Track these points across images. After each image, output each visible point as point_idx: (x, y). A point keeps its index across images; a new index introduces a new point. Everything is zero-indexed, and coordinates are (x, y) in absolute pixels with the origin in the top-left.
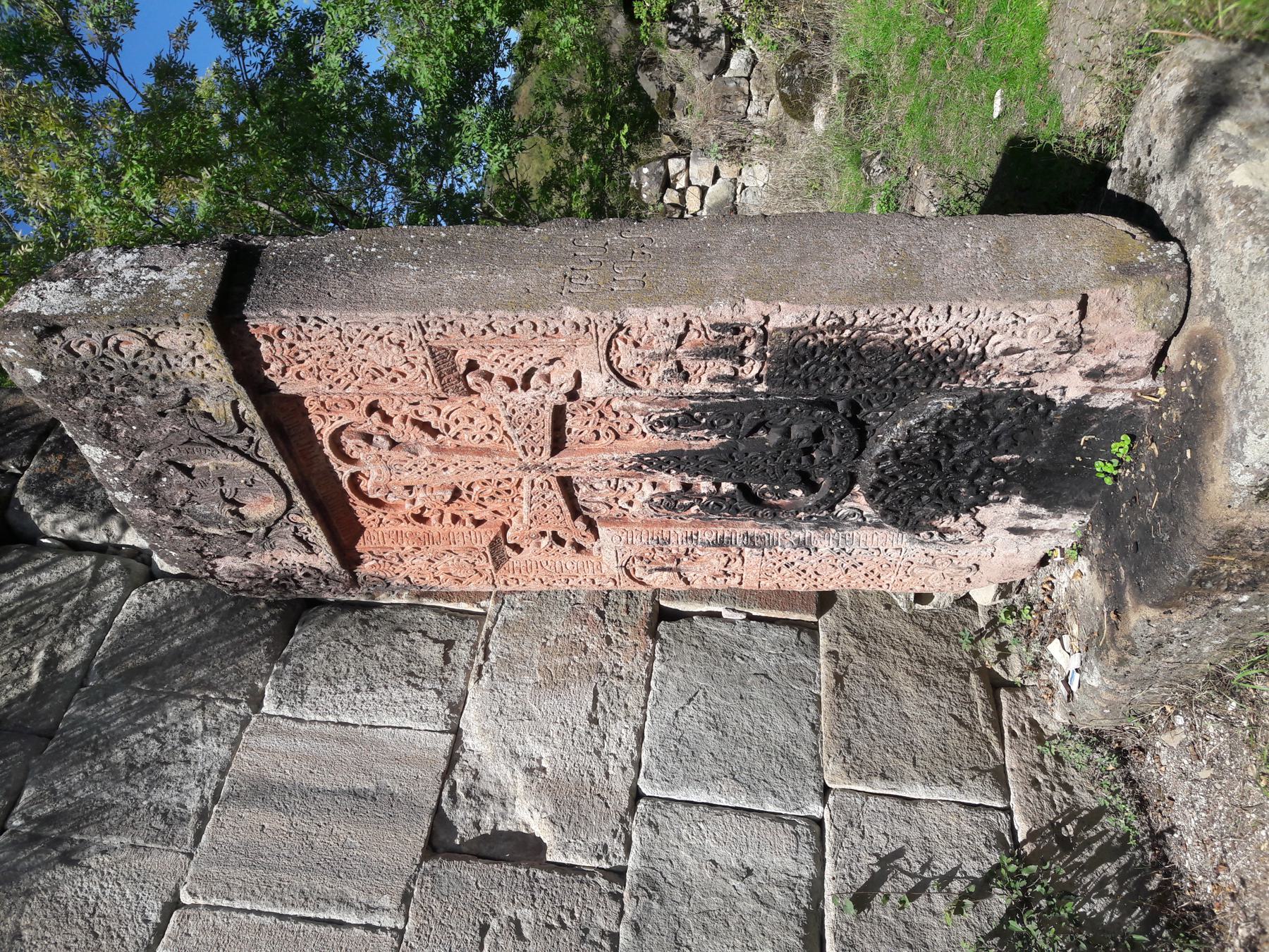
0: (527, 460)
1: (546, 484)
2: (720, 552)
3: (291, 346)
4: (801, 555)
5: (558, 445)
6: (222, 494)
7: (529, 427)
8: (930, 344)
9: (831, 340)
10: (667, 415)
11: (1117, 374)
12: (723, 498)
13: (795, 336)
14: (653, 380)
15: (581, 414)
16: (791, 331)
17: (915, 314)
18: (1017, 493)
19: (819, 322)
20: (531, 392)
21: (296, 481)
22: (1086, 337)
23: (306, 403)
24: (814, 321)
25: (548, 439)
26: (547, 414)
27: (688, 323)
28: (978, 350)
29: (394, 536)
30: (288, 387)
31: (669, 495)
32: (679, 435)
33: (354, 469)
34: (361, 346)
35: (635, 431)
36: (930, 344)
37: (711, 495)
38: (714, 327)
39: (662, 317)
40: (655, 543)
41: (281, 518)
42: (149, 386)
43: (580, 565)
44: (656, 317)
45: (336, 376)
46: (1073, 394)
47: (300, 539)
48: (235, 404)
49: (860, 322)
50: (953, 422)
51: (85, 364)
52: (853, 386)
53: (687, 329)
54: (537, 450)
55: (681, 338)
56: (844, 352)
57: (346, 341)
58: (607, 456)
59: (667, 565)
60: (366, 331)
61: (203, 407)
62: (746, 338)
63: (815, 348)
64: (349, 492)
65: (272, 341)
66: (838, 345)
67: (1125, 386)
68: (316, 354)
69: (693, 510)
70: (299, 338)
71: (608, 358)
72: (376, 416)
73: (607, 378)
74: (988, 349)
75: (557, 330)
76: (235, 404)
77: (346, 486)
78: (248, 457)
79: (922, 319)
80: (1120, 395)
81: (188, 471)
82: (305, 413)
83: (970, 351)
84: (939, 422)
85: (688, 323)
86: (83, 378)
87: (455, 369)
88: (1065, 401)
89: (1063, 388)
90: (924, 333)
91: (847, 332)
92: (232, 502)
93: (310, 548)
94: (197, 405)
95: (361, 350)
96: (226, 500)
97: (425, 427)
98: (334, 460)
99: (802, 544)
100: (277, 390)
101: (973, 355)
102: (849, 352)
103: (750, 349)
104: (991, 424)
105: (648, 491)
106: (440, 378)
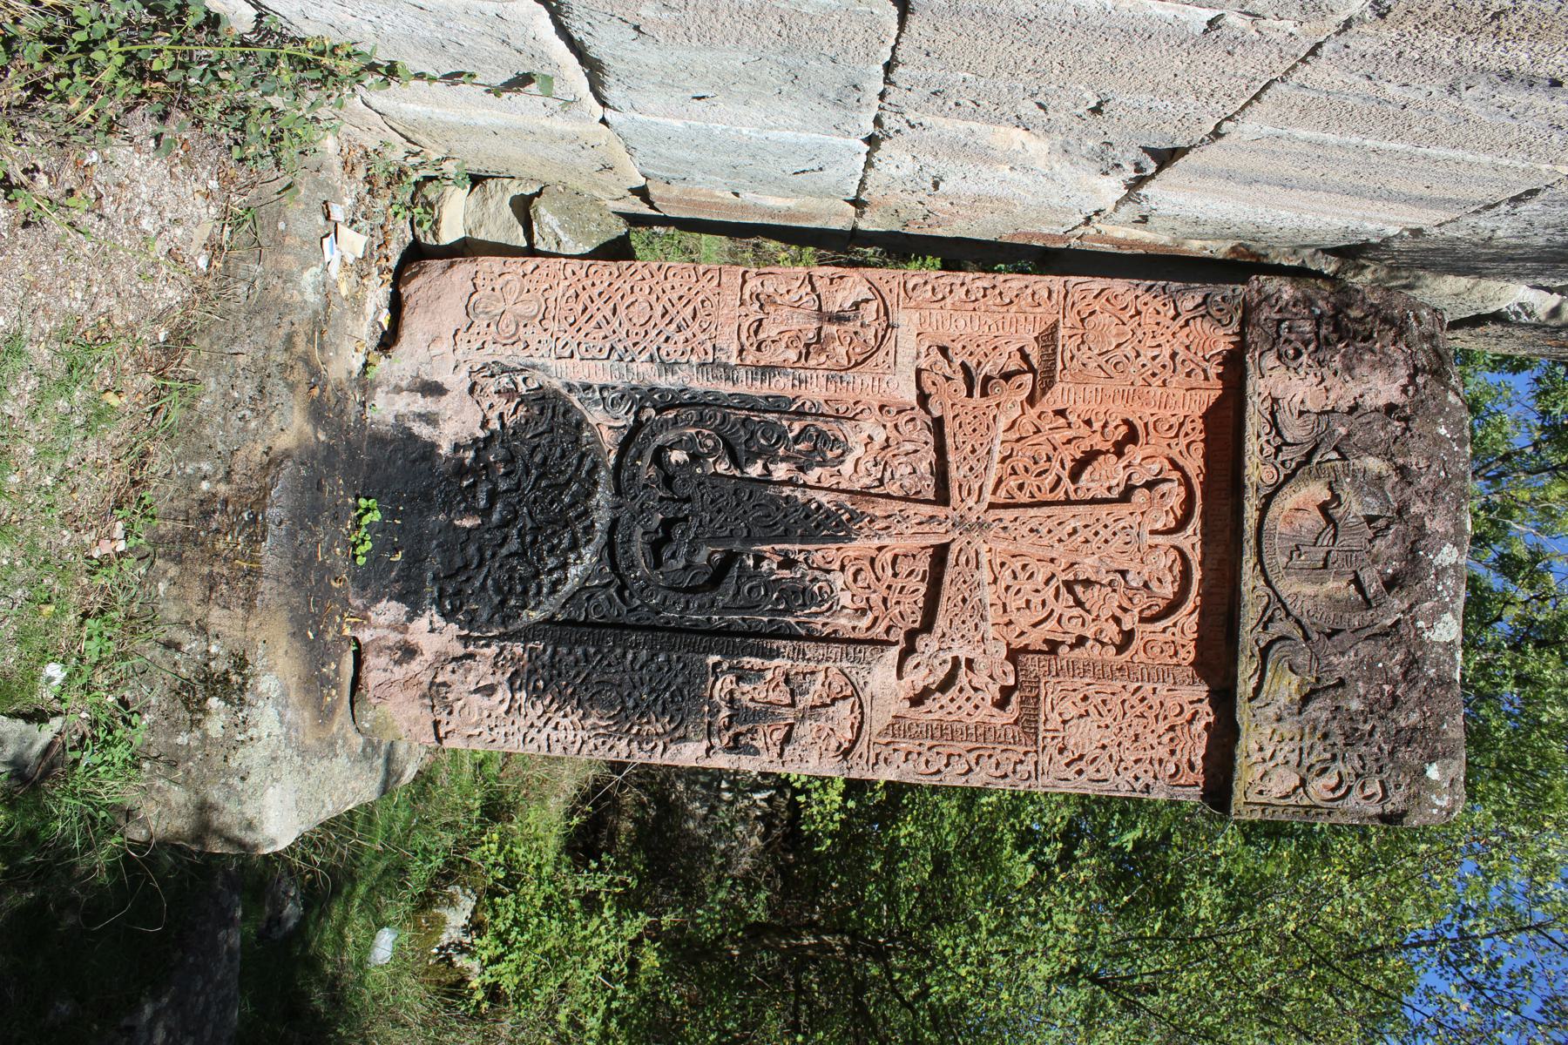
0: (978, 542)
1: (965, 493)
2: (766, 358)
3: (1173, 752)
4: (670, 347)
5: (940, 554)
6: (1335, 536)
7: (964, 600)
8: (558, 709)
9: (648, 722)
10: (814, 609)
11: (389, 648)
12: (758, 455)
13: (681, 731)
14: (820, 677)
15: (906, 608)
16: (684, 739)
17: (578, 745)
18: (448, 459)
19: (661, 748)
20: (949, 656)
21: (1240, 553)
22: (427, 701)
23: (1192, 656)
24: (665, 750)
25: (947, 579)
26: (941, 623)
27: (781, 755)
28: (518, 696)
29: (1171, 402)
30: (1202, 690)
31: (822, 464)
32: (803, 575)
33: (1178, 540)
34: (1104, 747)
35: (851, 571)
36: (558, 709)
37: (774, 458)
38: (757, 752)
39: (804, 765)
40: (846, 378)
41: (1288, 478)
42: (1335, 723)
43: (947, 324)
44: (810, 765)
45: (1140, 708)
46: (422, 623)
47: (1279, 433)
48: (1257, 690)
49: (624, 742)
50: (525, 591)
51: (1380, 770)
52: (624, 655)
53: (782, 750)
54: (963, 559)
55: (787, 739)
56: (636, 706)
57: (1116, 758)
58: (886, 541)
59: (835, 328)
60: (1092, 769)
61: (1295, 680)
62: (728, 728)
63: (663, 713)
64: (1198, 493)
65: (1189, 760)
66: (642, 715)
67: (380, 632)
68: (1153, 740)
69: (797, 427)
70: (1161, 761)
71: (862, 713)
72: (1126, 627)
73: (868, 690)
74: (509, 695)
75: (907, 760)
76: (1257, 690)
77: (1196, 522)
78: (1280, 600)
79: (570, 738)
80: (382, 620)
81: (1357, 581)
82: (1199, 642)
83: (524, 694)
84: (539, 592)
85: (781, 755)
86: (1392, 753)
87: (1022, 702)
88: (428, 613)
89: (432, 631)
90: (566, 722)
91: (634, 731)
92: (1330, 519)
93: (1273, 414)
94: (1300, 686)
95: (1105, 741)
96: (1335, 526)
97: (1079, 603)
98: (1195, 557)
99: (669, 367)
100: (1211, 693)
101: (520, 689)
102: (630, 704)
103: (725, 712)
104: (490, 582)
105: (847, 468)
106: (1037, 696)
